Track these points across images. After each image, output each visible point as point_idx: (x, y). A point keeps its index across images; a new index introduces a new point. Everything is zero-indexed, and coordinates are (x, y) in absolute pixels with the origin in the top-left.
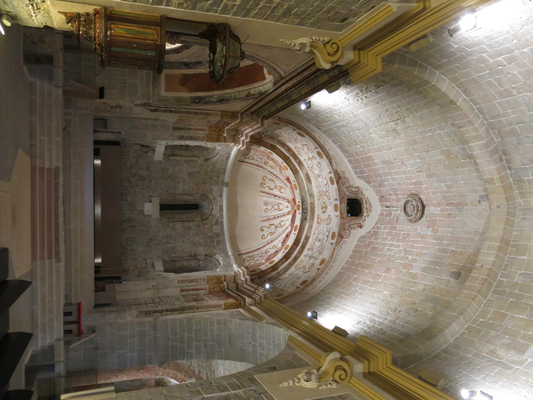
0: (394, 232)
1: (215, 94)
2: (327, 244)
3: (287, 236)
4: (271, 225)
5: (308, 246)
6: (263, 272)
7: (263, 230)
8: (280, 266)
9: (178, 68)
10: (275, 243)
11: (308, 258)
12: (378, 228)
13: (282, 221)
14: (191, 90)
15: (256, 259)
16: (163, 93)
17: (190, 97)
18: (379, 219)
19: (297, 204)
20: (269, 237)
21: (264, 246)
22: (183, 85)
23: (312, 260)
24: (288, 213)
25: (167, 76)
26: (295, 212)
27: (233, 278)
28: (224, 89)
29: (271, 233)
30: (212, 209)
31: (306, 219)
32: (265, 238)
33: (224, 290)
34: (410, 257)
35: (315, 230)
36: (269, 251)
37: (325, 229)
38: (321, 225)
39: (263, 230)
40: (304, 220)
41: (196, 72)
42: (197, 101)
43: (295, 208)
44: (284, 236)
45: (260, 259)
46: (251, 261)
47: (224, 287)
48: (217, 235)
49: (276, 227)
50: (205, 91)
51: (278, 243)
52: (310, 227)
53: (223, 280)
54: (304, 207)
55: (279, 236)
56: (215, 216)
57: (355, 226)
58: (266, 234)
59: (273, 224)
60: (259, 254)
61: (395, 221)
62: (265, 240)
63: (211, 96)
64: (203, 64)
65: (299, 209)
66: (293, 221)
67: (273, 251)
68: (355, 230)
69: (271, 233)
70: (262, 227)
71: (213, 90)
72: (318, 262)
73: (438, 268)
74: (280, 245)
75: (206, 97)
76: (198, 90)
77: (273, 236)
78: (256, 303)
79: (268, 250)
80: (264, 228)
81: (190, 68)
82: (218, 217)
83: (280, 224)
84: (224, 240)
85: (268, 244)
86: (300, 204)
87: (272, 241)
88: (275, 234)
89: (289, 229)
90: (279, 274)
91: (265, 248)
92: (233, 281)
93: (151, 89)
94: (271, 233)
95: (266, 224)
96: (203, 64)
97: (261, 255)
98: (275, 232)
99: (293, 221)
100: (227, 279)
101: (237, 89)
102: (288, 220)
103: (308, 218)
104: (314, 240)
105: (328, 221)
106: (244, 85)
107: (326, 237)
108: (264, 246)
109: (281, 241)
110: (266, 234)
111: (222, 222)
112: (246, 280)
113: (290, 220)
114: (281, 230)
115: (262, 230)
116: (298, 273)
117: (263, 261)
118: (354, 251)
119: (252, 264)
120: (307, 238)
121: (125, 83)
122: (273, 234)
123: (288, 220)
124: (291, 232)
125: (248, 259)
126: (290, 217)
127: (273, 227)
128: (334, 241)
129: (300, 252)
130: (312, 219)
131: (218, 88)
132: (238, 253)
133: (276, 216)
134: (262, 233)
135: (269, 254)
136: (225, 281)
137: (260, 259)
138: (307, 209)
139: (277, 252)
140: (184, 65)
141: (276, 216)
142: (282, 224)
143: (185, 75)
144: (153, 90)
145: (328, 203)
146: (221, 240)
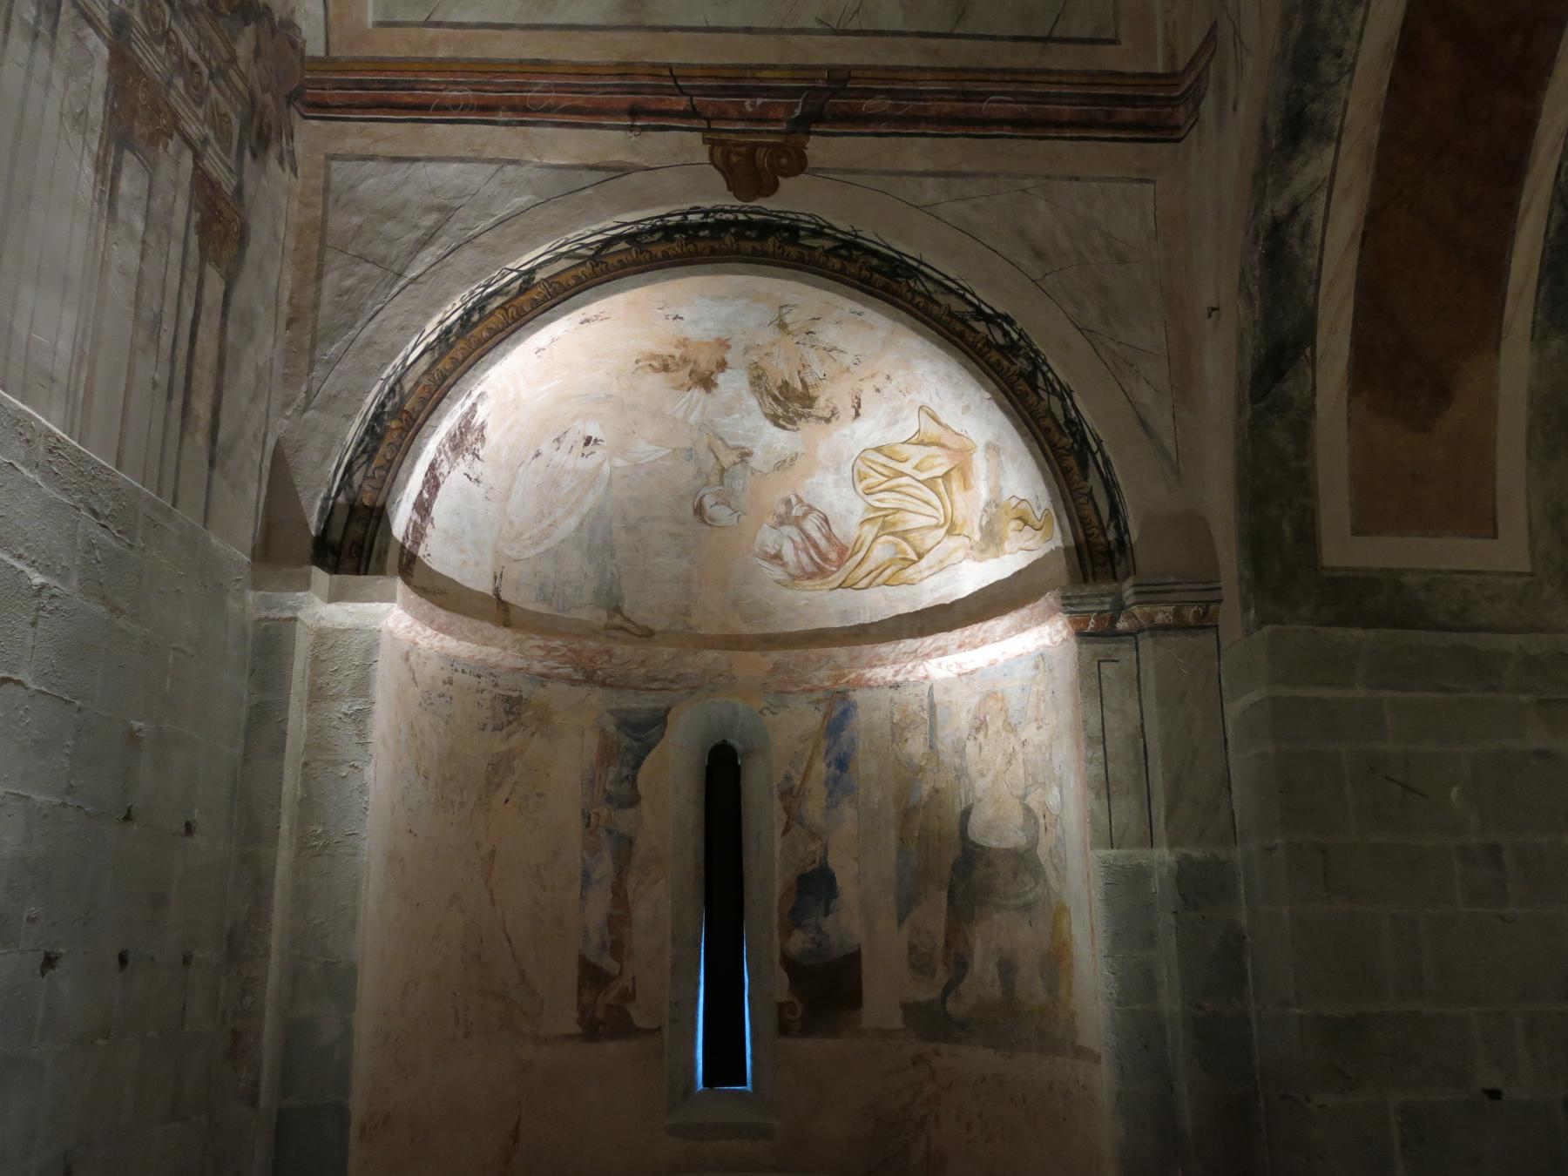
9: (1302, 432)
16: (1508, 551)
17: (1538, 338)
22: (1442, 393)
25: (1365, 524)
50: (1509, 210)
64: (1294, 210)
71: (1526, 127)
76: (1491, 269)
81: (1307, 331)
93: (1512, 643)
96: (1294, 210)
121: (1495, 850)
140: (1279, 376)
143: (1368, 367)
144: (1491, 628)
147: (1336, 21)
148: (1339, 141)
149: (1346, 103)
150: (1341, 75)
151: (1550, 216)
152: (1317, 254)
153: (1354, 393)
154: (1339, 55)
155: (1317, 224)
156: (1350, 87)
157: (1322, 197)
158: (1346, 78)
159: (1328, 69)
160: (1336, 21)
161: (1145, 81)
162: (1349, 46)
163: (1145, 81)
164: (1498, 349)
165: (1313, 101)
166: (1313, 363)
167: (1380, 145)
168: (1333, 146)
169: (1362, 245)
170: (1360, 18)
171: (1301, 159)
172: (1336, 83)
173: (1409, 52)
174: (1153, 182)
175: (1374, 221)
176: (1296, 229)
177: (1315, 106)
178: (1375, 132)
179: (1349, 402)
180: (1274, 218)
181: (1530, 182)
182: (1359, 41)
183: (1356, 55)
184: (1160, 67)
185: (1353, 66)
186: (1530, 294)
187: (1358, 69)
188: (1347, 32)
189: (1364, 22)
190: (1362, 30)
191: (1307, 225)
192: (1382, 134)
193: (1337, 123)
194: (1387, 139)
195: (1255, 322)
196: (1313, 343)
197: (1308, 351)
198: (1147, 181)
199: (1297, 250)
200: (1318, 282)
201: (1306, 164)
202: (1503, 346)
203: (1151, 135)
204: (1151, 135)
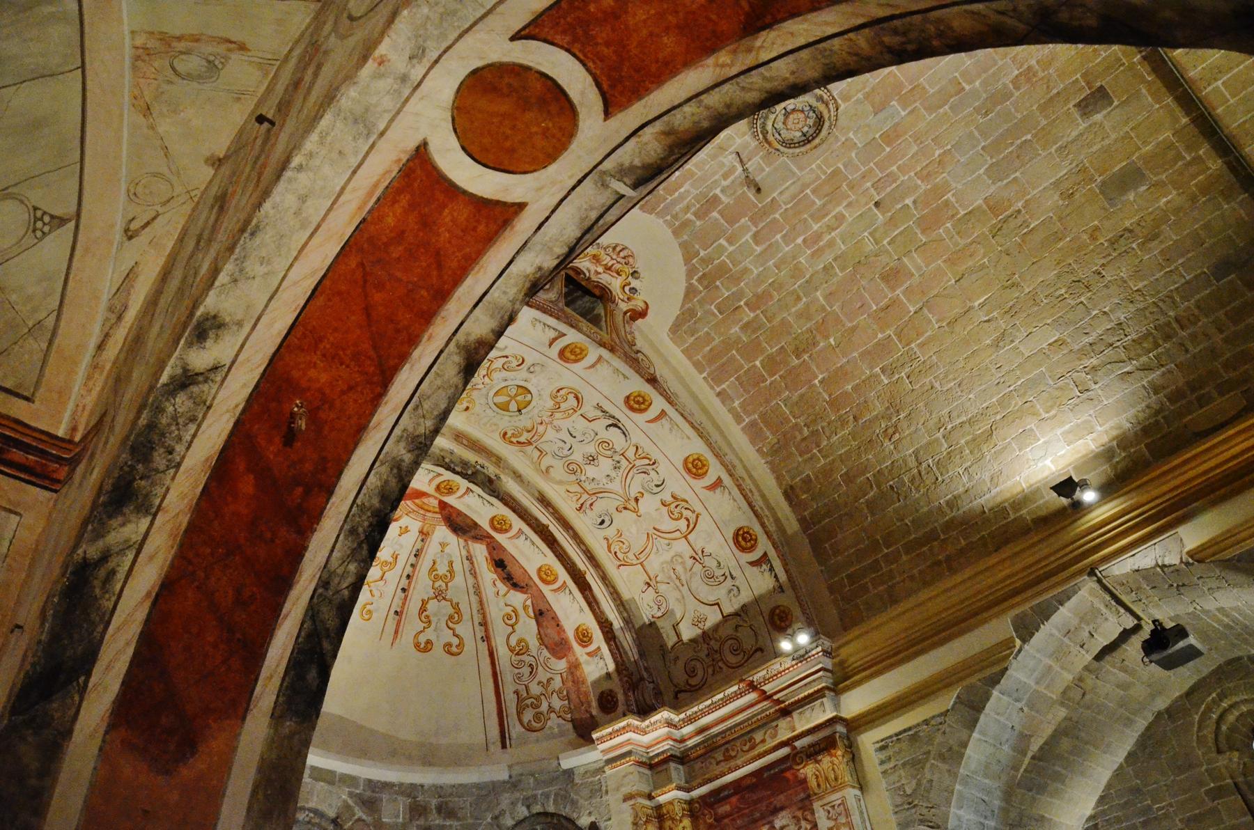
0: (777, 216)
1: (321, 558)
2: (636, 437)
3: (500, 564)
4: (423, 609)
5: (568, 508)
6: (618, 670)
7: (428, 642)
8: (602, 613)
10: (496, 612)
11: (624, 521)
12: (706, 261)
13: (433, 569)
14: (239, 704)
15: (535, 689)
17: (277, 716)
18: (684, 246)
19: (430, 490)
20: (464, 629)
21: (491, 655)
22: (189, 744)
23: (649, 505)
24: (424, 535)
26: (443, 505)
27: (642, 770)
28: (330, 492)
29: (455, 617)
30: (315, 812)
31: (490, 481)
32: (461, 645)
33: (690, 802)
34: (909, 201)
35: (537, 465)
36: (520, 641)
37: (580, 425)
38: (551, 434)
39: (428, 642)
40: (491, 486)
41: (135, 629)
42: (312, 674)
43: (435, 503)
44: (488, 575)
45: (542, 675)
46: (544, 707)
47: (680, 801)
48: (417, 810)
49: (439, 595)
51: (502, 601)
52: (518, 477)
53: (647, 803)
54: (458, 469)
55: (478, 592)
56: (345, 801)
57: (628, 329)
58: (447, 636)
59: (424, 603)
60: (519, 677)
61: (751, 195)
62: (469, 645)
63: (324, 583)
64: (105, 557)
65: (450, 491)
66: (460, 525)
67: (528, 629)
68: (637, 334)
69: (455, 617)
70: (417, 645)
71: (296, 555)
72: (679, 484)
73: (1029, 137)
74: (517, 598)
75: (312, 612)
77: (466, 616)
78: (833, 690)
79: (513, 642)
80: (422, 639)
82: (351, 795)
83: (437, 578)
84: (438, 790)
85: (487, 638)
86: (448, 475)
87: (484, 624)
88: (464, 607)
89: (480, 551)
90: (628, 621)
91: (502, 652)
92: (647, 772)
94: (451, 617)
95: (412, 625)
96: (105, 557)
97: (526, 670)
98: (456, 607)
99: (460, 525)
100: (645, 789)
101: (385, 415)
102: (443, 545)
103: (491, 470)
104: (573, 478)
105: (572, 402)
106: (403, 358)
107: (614, 435)
108: (491, 655)
109: (503, 588)
110: (447, 636)
111: (370, 783)
112: (670, 724)
113: (451, 538)
114: (459, 580)
115: (427, 647)
116: (667, 556)
117: (561, 665)
118: (698, 366)
119: (557, 703)
120: (544, 501)
122: (458, 611)
123: (443, 545)
124: (493, 547)
125: (528, 716)
126: (442, 532)
127: (432, 606)
128: (659, 404)
129: (576, 537)
130: (499, 461)
131: (305, 520)
132: (496, 747)
133: (404, 582)
134: (438, 649)
135: (533, 643)
136: (650, 797)
137: (542, 675)
138: (465, 464)
139: (542, 614)
141: (404, 582)
142: (442, 569)
145: (519, 377)
146: (434, 802)
147: (173, 428)
148: (155, 515)
149: (168, 489)
150: (168, 468)
151: (302, 625)
152: (114, 599)
153: (112, 727)
154: (170, 453)
155: (121, 576)
156: (173, 478)
157: (130, 556)
158: (172, 471)
159: (159, 459)
160: (173, 428)
161: (43, 437)
162: (179, 448)
163: (43, 437)
164: (244, 719)
165: (141, 479)
166: (83, 691)
167: (186, 531)
168: (149, 519)
169: (154, 604)
170: (192, 432)
171: (120, 519)
172: (163, 472)
173: (222, 470)
174: (20, 515)
175: (167, 589)
176: (102, 573)
177: (143, 483)
178: (185, 521)
179: (106, 733)
180: (84, 559)
181: (293, 594)
182: (188, 448)
183: (183, 457)
184: (60, 433)
185: (178, 465)
186: (276, 682)
187: (182, 469)
188: (180, 439)
189: (194, 436)
190: (191, 442)
191: (113, 572)
192: (189, 523)
193: (157, 502)
194: (192, 529)
195: (39, 642)
196: (88, 675)
197: (82, 679)
198: (16, 513)
199: (97, 591)
200: (108, 623)
201: (123, 525)
202: (248, 718)
203: (33, 479)
204: (33, 479)
